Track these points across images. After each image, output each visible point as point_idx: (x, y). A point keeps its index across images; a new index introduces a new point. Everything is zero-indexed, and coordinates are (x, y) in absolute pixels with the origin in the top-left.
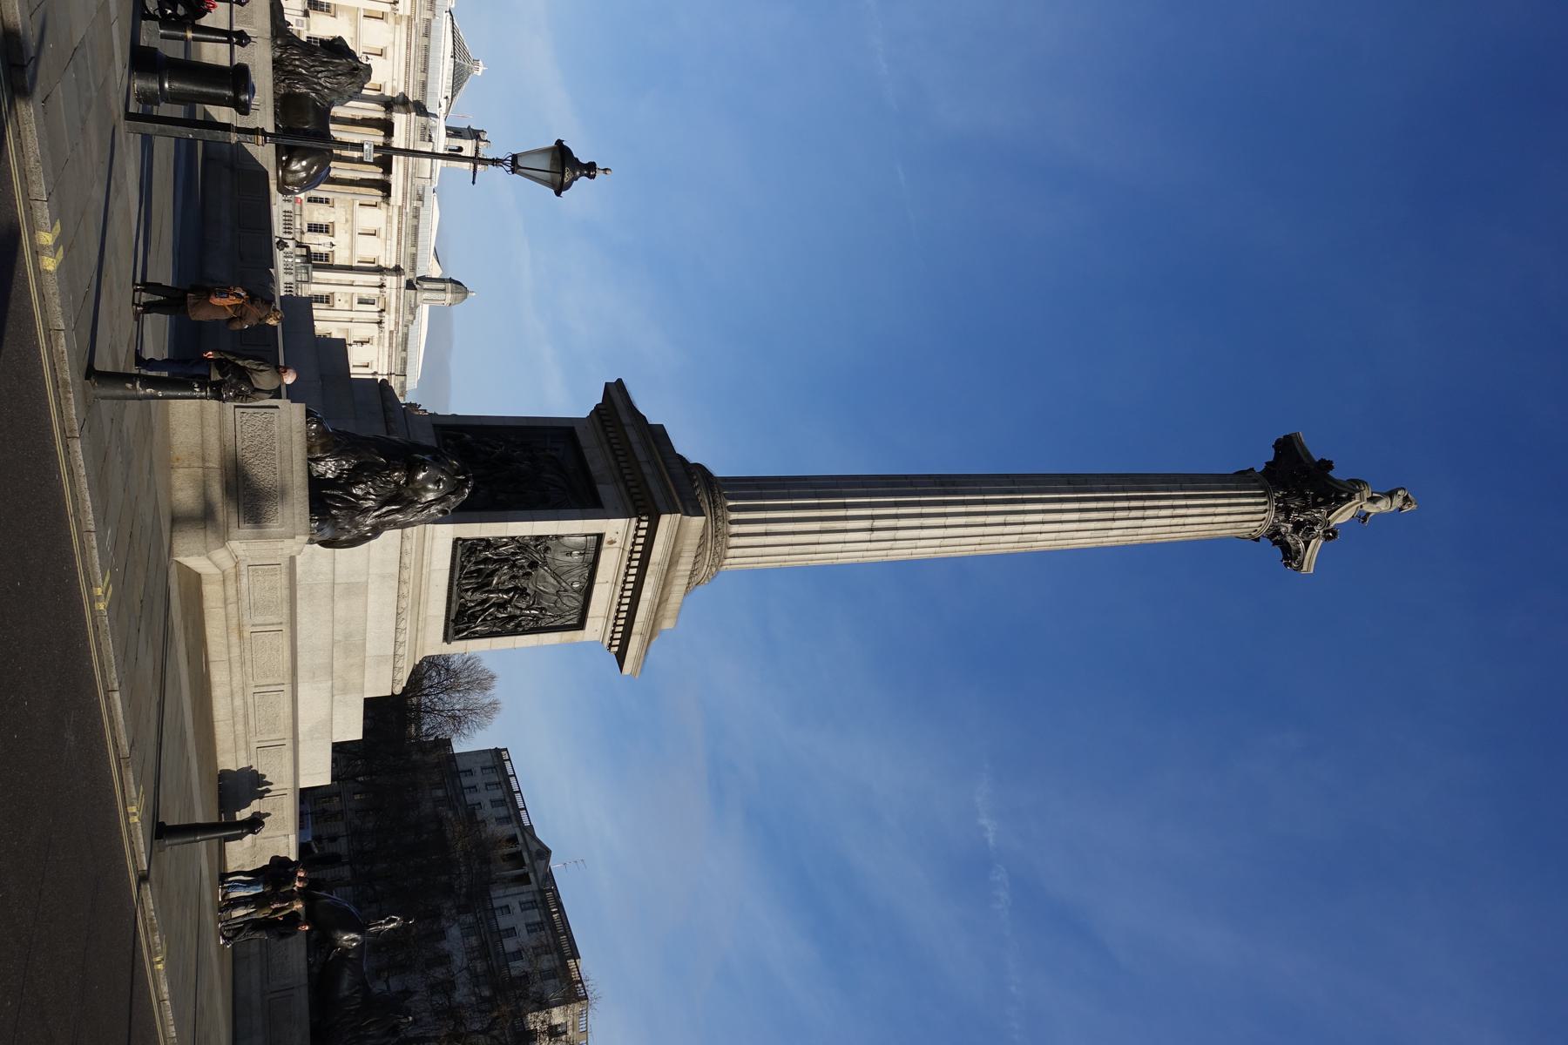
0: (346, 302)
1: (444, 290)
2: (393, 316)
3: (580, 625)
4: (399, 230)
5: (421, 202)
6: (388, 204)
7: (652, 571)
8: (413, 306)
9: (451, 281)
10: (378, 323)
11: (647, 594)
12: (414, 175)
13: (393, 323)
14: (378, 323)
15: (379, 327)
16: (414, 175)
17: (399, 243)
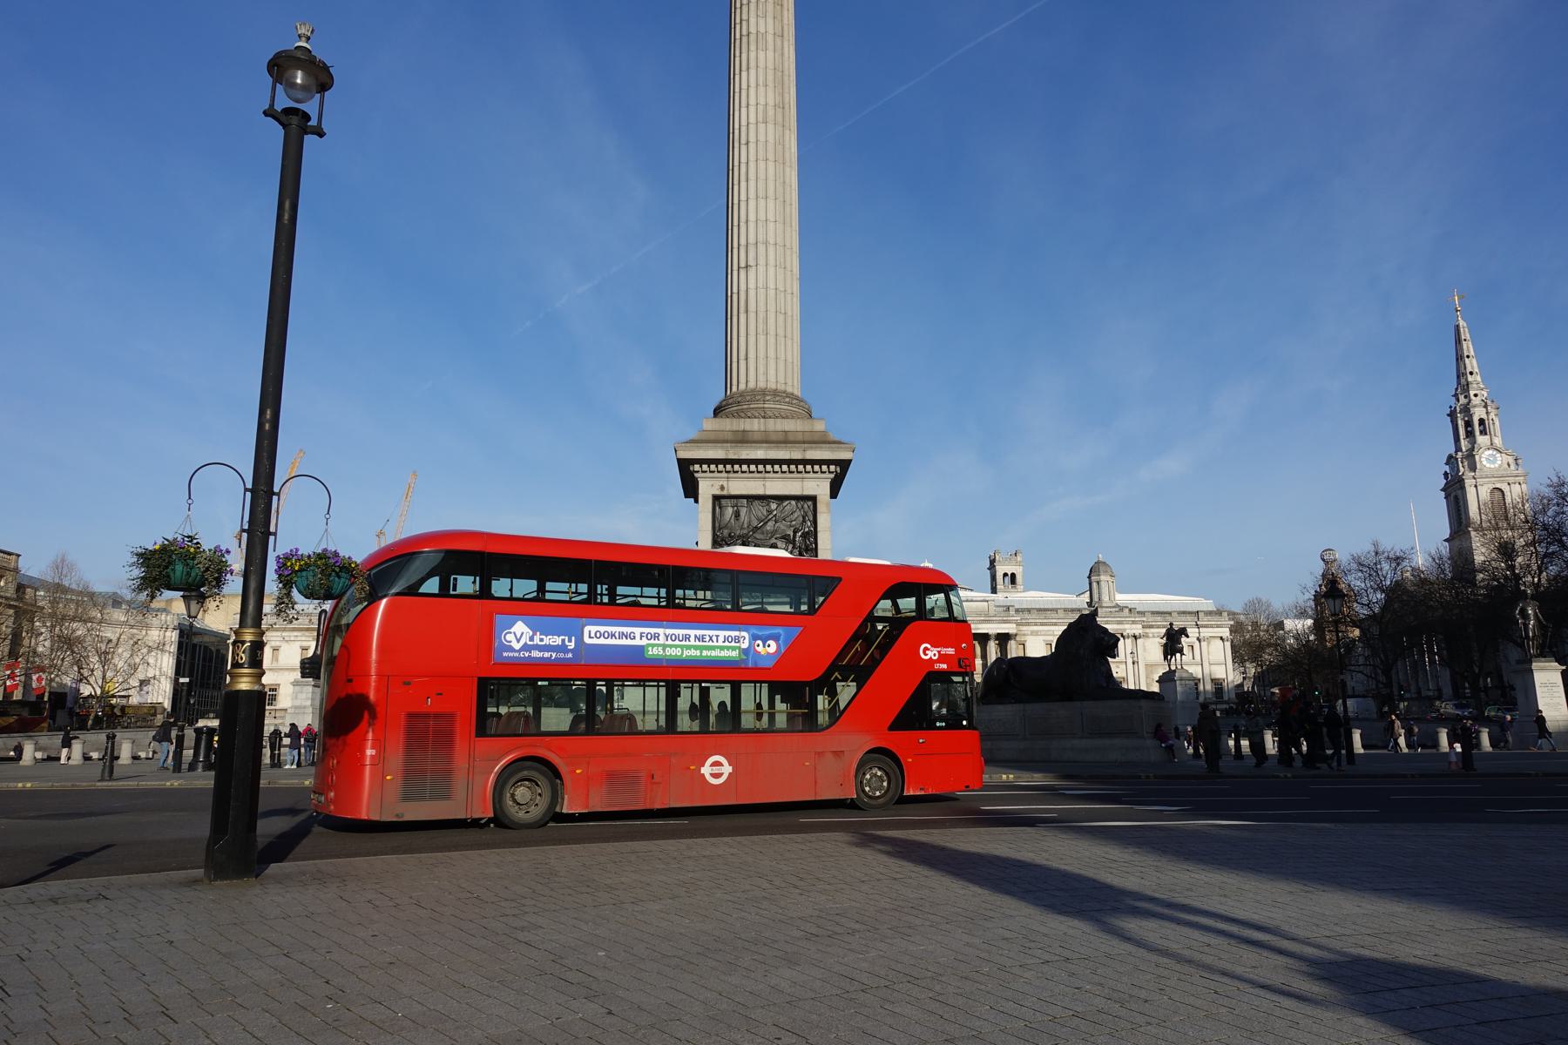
0: (1118, 667)
1: (1098, 583)
2: (1127, 626)
3: (813, 499)
4: (1042, 624)
5: (1011, 608)
6: (1016, 635)
7: (735, 454)
8: (1117, 609)
9: (1089, 577)
10: (1136, 639)
11: (760, 454)
12: (986, 616)
13: (1134, 626)
14: (1136, 639)
15: (1140, 637)
16: (986, 616)
17: (1055, 624)
